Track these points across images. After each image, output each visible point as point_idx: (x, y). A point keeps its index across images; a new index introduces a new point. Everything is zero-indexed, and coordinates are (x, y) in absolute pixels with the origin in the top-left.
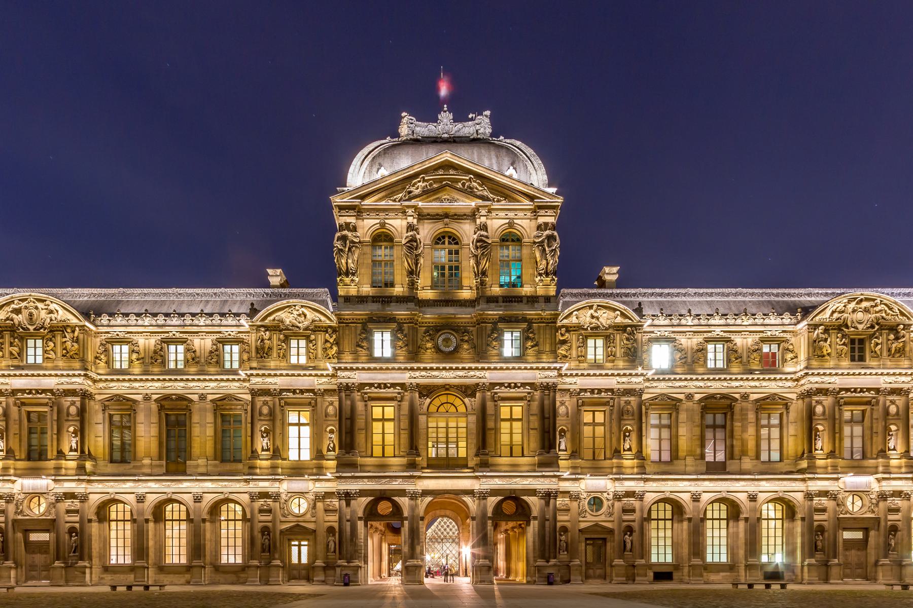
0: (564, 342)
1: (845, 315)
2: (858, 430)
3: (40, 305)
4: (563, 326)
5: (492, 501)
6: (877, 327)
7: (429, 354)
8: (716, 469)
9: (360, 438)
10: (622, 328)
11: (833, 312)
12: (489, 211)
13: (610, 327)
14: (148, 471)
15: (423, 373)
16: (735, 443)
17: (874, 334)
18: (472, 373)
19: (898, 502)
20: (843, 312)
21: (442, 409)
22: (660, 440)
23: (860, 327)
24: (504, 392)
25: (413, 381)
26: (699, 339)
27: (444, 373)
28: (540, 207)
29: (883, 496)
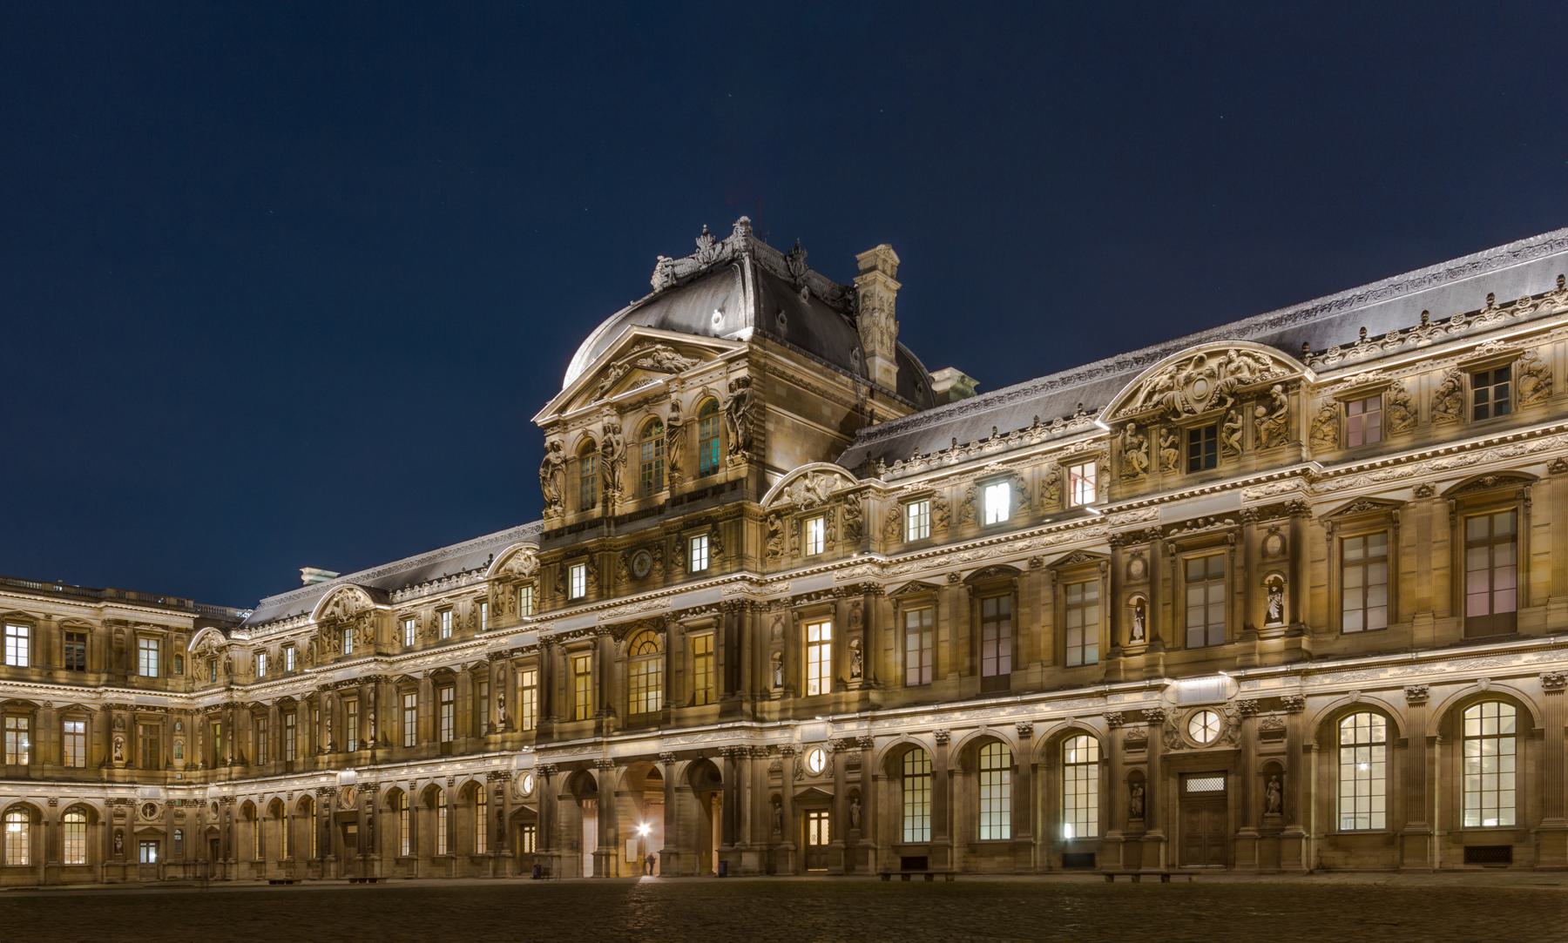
0: (774, 534)
1: (1170, 394)
2: (1218, 591)
3: (350, 594)
4: (773, 512)
5: (682, 765)
6: (1230, 401)
7: (624, 585)
8: (997, 688)
9: (558, 701)
10: (840, 497)
11: (1150, 395)
12: (683, 382)
13: (829, 498)
14: (424, 754)
15: (612, 611)
16: (1020, 641)
17: (1228, 410)
18: (657, 602)
19: (1282, 718)
20: (1169, 388)
21: (643, 651)
22: (921, 650)
23: (1199, 408)
24: (692, 620)
25: (602, 623)
26: (966, 483)
27: (630, 608)
28: (731, 361)
29: (1248, 710)
